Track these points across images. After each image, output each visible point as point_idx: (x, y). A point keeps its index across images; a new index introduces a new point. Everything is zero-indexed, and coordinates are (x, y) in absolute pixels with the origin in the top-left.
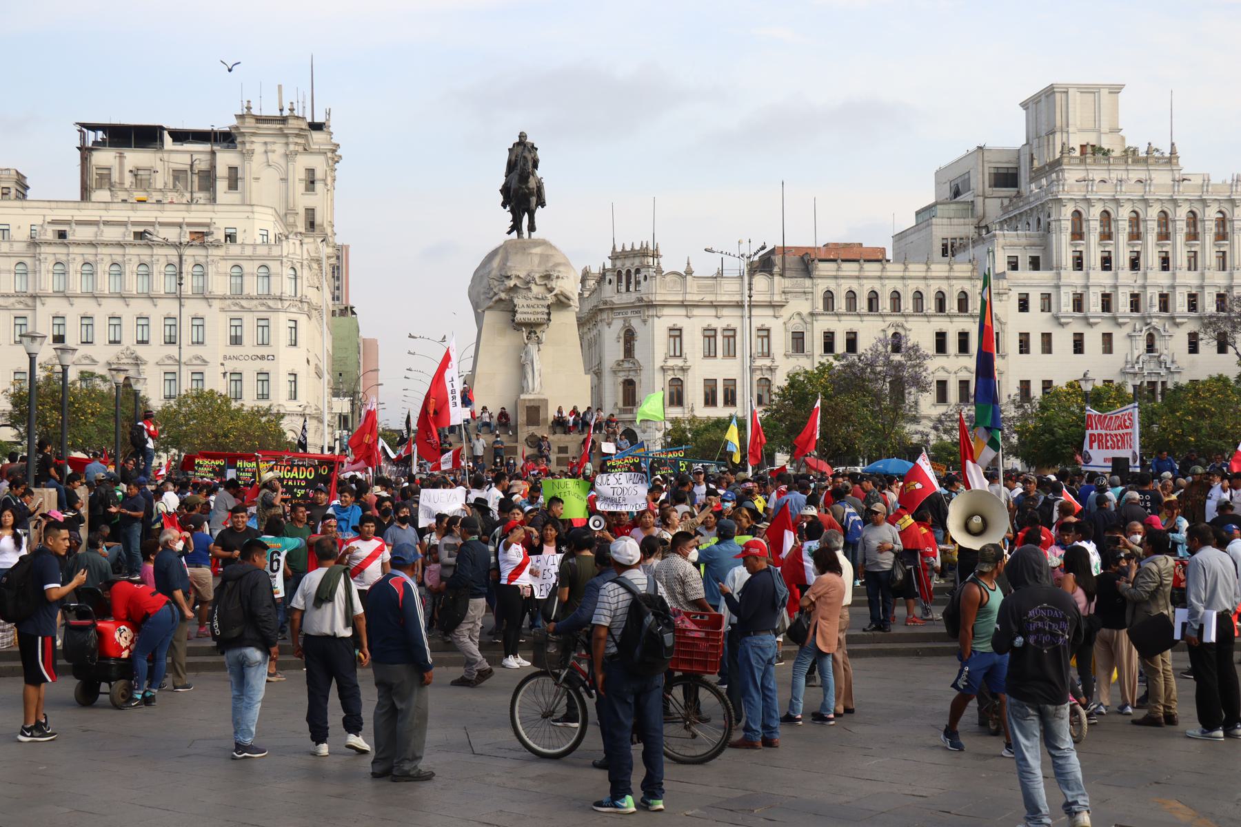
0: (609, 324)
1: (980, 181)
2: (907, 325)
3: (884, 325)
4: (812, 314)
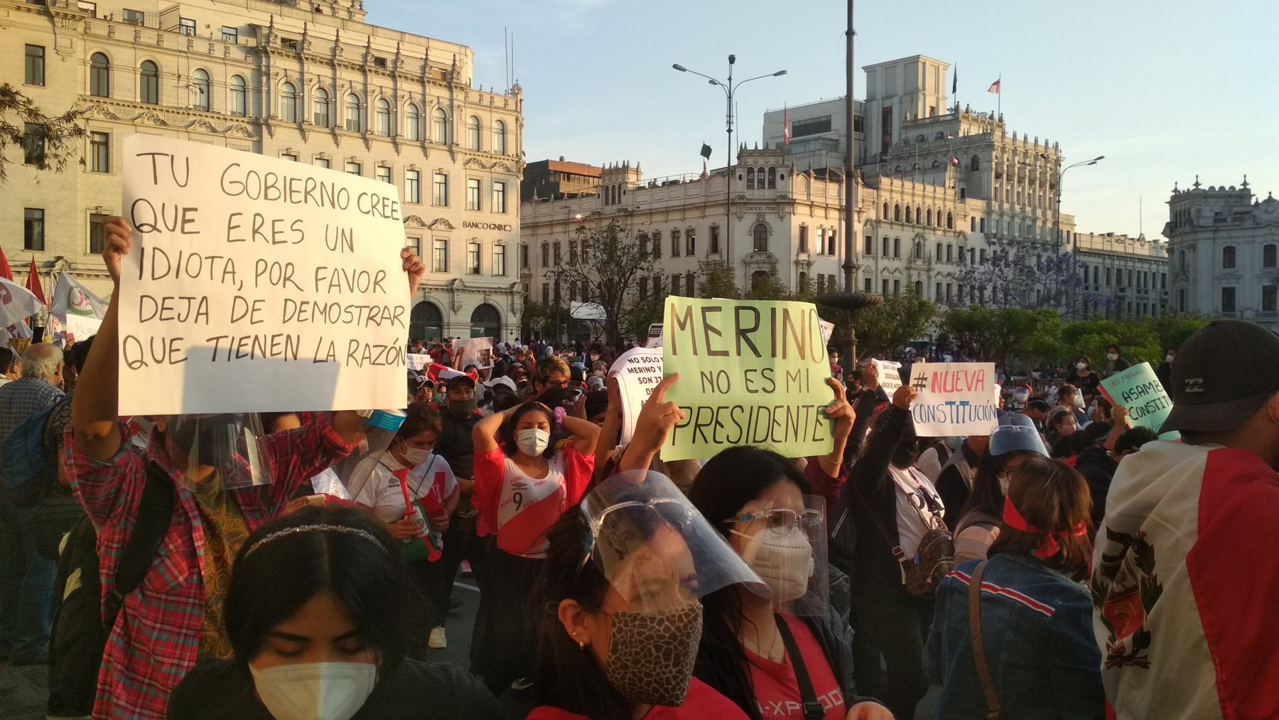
0: (740, 218)
1: (839, 124)
2: (926, 236)
3: (912, 235)
4: (878, 222)
